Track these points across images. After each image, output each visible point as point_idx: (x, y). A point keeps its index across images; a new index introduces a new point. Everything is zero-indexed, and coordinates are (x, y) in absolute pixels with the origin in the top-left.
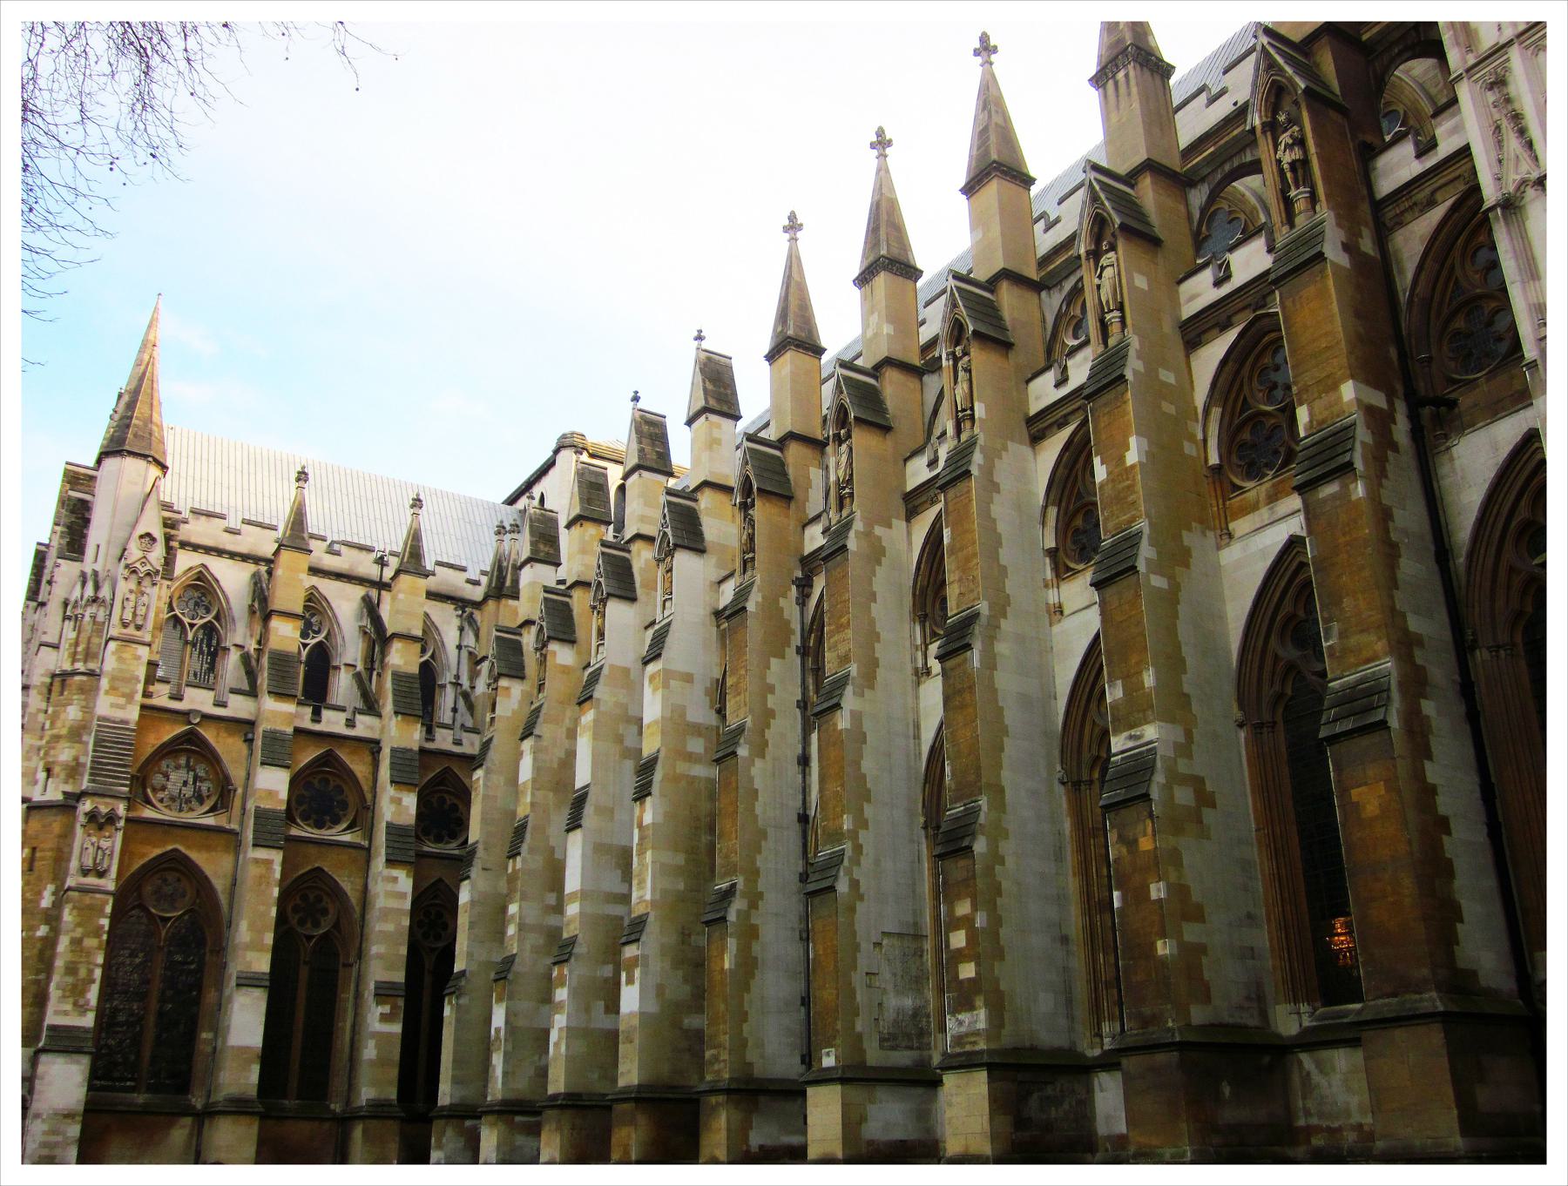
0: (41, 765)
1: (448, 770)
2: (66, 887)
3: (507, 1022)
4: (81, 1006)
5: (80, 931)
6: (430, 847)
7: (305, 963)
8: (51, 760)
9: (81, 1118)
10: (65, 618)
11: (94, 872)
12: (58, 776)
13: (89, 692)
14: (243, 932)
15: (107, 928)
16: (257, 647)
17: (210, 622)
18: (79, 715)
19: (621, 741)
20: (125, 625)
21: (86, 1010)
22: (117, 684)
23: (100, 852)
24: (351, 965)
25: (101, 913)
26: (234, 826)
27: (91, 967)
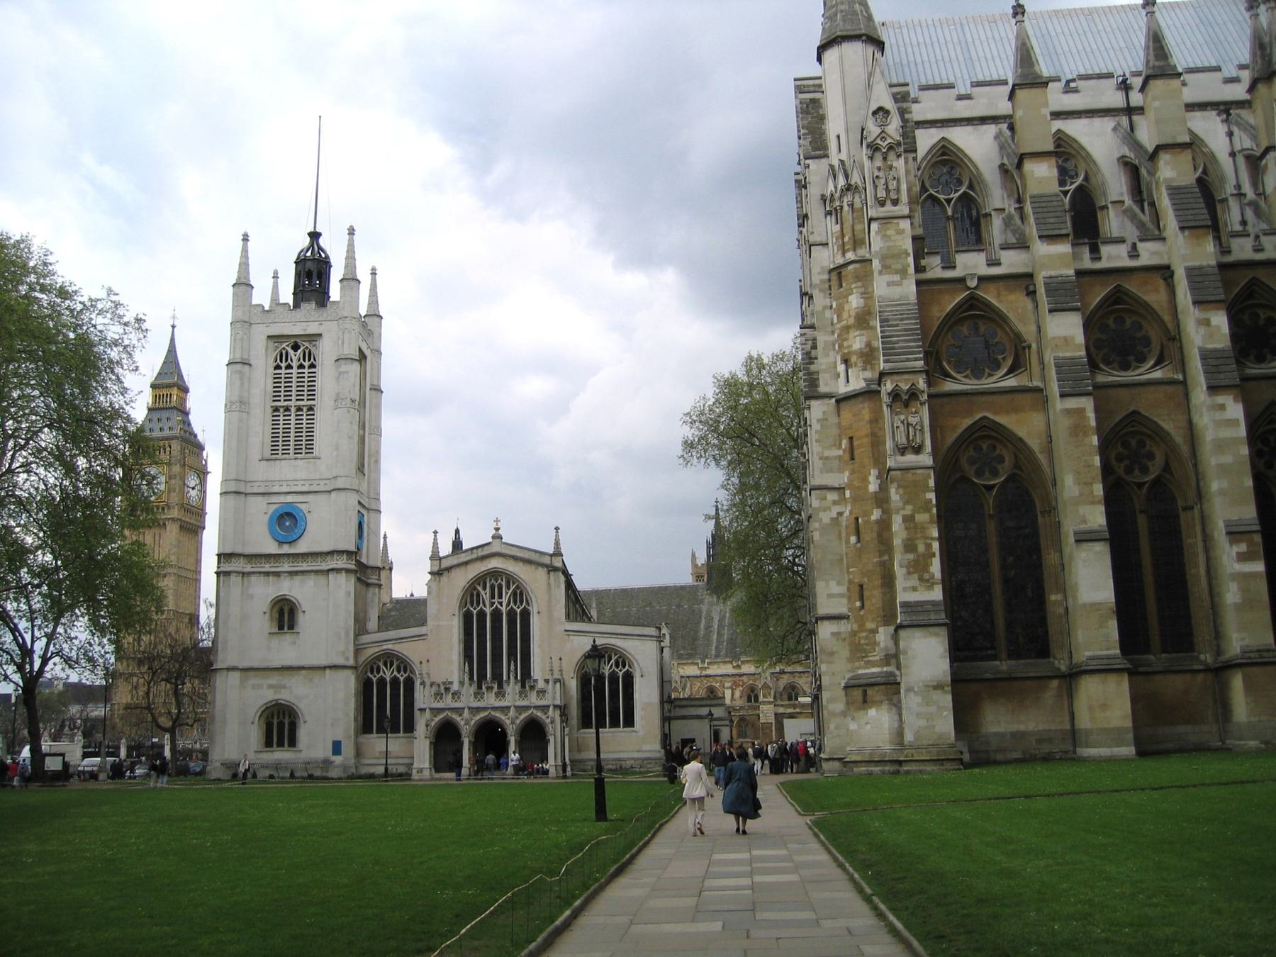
1: (1254, 282)
4: (928, 581)
6: (1253, 370)
7: (1141, 512)
8: (846, 351)
9: (950, 688)
11: (910, 449)
12: (856, 365)
13: (865, 277)
14: (1069, 486)
15: (934, 502)
16: (1017, 206)
17: (965, 193)
20: (882, 203)
21: (933, 584)
22: (889, 262)
24: (1192, 508)
25: (927, 489)
26: (1037, 383)
27: (929, 541)
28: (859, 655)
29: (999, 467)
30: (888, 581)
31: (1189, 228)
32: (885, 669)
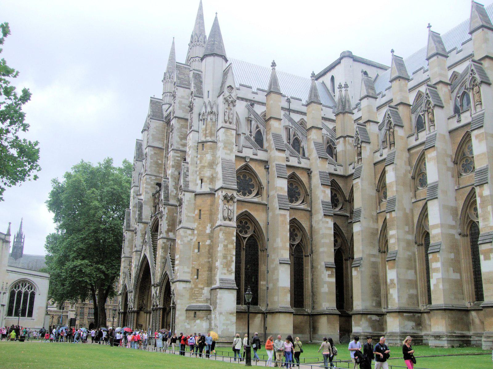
0: (198, 178)
2: (217, 225)
3: (397, 277)
5: (226, 242)
8: (202, 175)
9: (236, 314)
10: (200, 120)
12: (206, 182)
15: (235, 241)
16: (250, 134)
18: (212, 158)
19: (446, 165)
21: (232, 273)
23: (229, 211)
26: (265, 202)
27: (232, 256)
28: (193, 298)
29: (248, 230)
30: (211, 269)
31: (322, 158)
32: (206, 304)
